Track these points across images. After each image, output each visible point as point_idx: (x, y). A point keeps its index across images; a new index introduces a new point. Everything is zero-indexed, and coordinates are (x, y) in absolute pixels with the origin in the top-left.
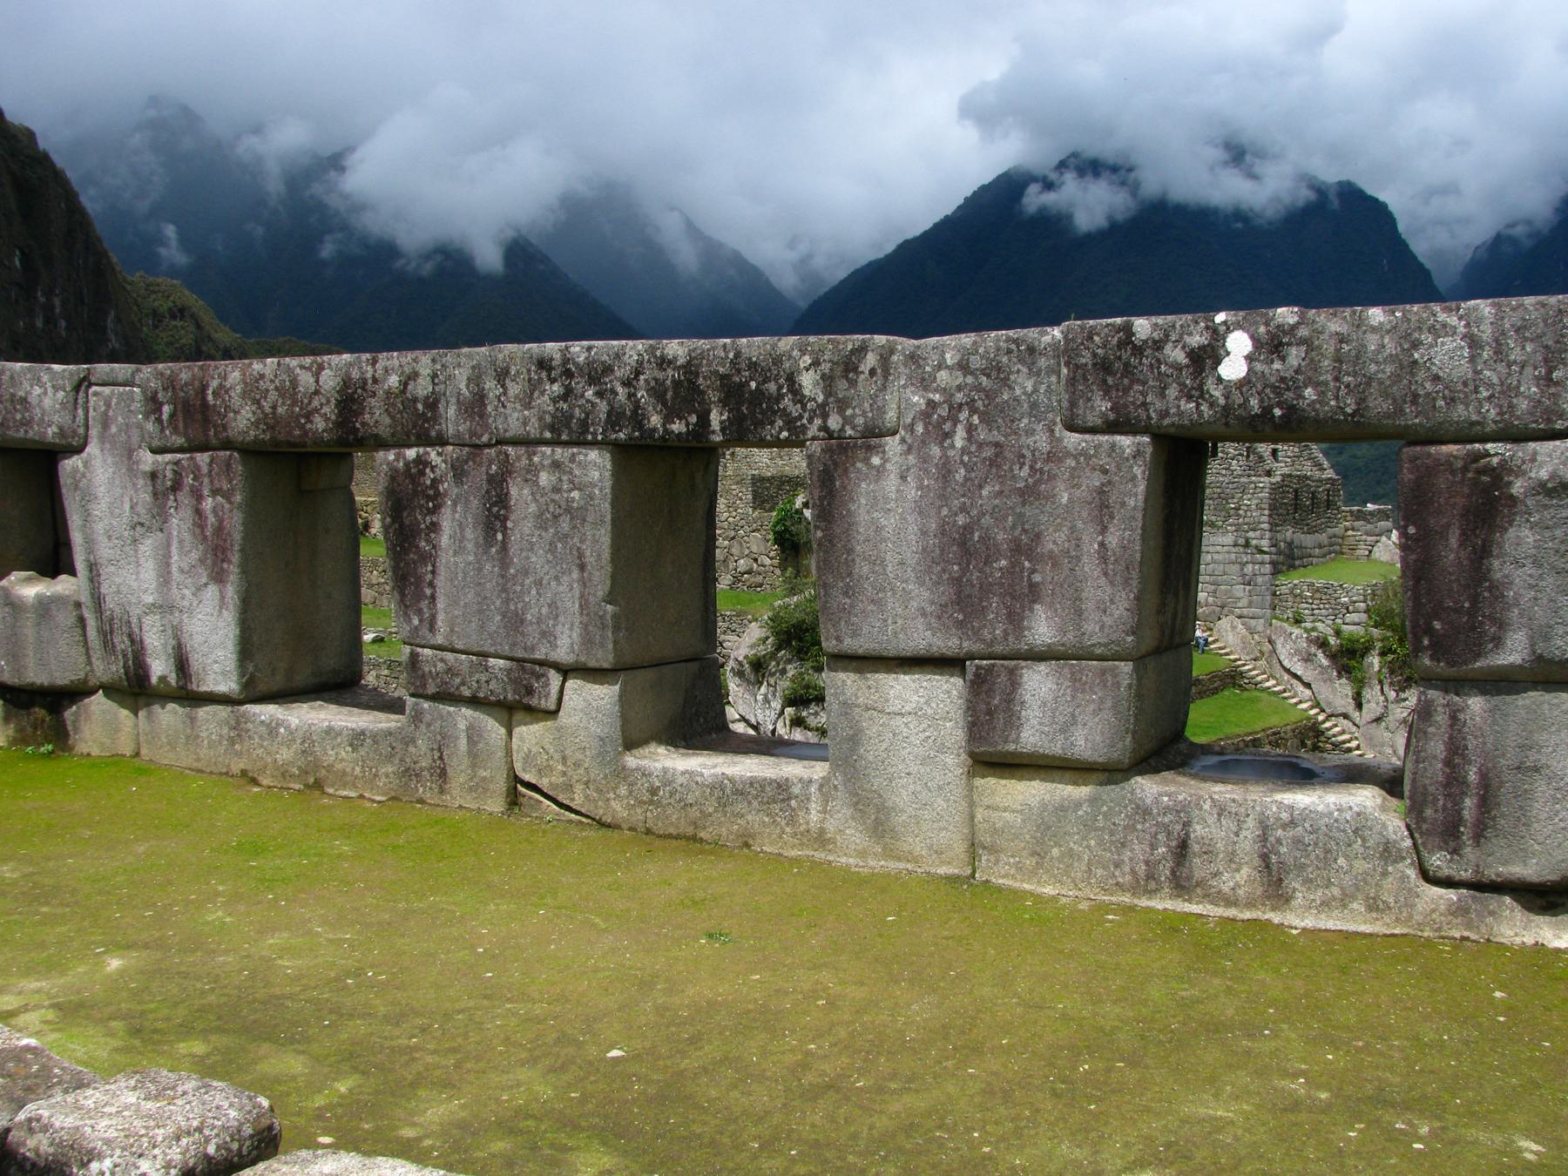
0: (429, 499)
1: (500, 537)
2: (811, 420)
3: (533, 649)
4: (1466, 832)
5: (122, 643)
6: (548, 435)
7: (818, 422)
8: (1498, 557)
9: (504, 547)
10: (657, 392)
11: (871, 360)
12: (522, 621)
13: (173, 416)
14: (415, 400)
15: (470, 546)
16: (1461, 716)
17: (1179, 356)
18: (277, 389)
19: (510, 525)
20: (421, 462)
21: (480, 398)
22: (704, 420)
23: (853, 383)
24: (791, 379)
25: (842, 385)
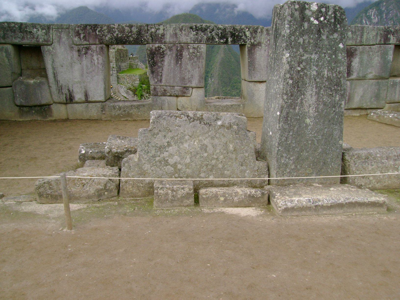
1: (180, 62)
3: (187, 84)
5: (65, 91)
6: (192, 42)
10: (218, 35)
11: (259, 30)
12: (184, 79)
13: (84, 37)
14: (159, 34)
15: (172, 65)
18: (118, 31)
20: (160, 48)
21: (176, 34)
23: (256, 34)
24: (244, 32)
25: (254, 35)
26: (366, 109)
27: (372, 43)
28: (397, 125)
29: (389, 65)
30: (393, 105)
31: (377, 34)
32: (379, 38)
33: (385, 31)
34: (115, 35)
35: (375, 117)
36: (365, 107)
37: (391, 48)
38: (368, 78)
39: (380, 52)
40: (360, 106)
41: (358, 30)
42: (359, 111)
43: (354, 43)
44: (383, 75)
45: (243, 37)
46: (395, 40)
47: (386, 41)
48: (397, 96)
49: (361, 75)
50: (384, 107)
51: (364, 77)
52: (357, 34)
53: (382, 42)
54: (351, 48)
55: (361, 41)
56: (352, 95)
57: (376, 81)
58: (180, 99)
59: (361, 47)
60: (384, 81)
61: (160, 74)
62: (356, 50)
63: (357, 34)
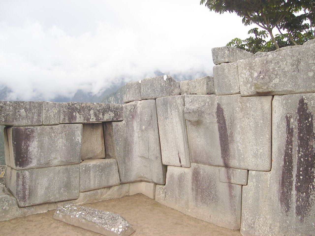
4: (27, 197)
8: (31, 147)
16: (25, 176)
26: (56, 202)
27: (53, 123)
28: (85, 228)
29: (78, 148)
30: (89, 193)
31: (59, 111)
32: (62, 117)
33: (69, 108)
35: (61, 216)
36: (53, 200)
37: (77, 127)
38: (53, 165)
39: (64, 133)
40: (46, 200)
41: (34, 107)
42: (47, 206)
43: (30, 123)
44: (72, 160)
46: (82, 118)
47: (71, 120)
48: (92, 183)
49: (42, 162)
50: (79, 196)
51: (48, 163)
52: (33, 111)
53: (67, 122)
54: (26, 129)
55: (39, 120)
56: (34, 188)
57: (64, 167)
59: (39, 128)
60: (73, 167)
62: (33, 131)
63: (33, 111)
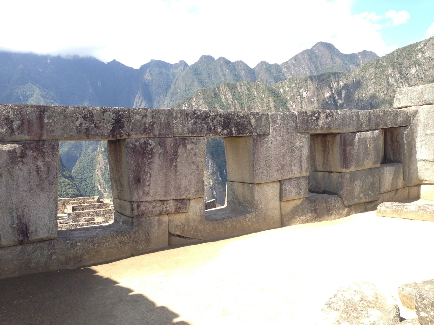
0: (149, 154)
1: (174, 164)
2: (253, 131)
7: (255, 131)
9: (176, 166)
13: (20, 127)
17: (314, 118)
19: (178, 160)
22: (231, 130)
34: (78, 124)
45: (249, 126)
58: (172, 217)
61: (147, 184)
